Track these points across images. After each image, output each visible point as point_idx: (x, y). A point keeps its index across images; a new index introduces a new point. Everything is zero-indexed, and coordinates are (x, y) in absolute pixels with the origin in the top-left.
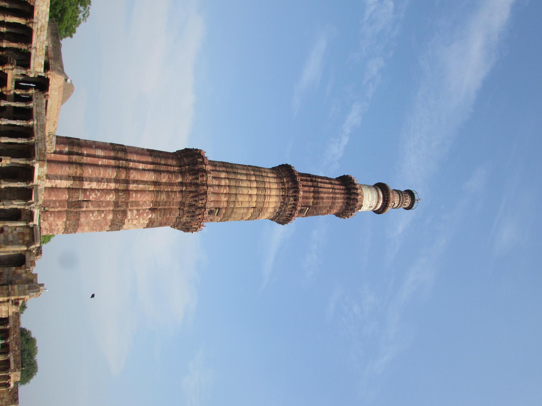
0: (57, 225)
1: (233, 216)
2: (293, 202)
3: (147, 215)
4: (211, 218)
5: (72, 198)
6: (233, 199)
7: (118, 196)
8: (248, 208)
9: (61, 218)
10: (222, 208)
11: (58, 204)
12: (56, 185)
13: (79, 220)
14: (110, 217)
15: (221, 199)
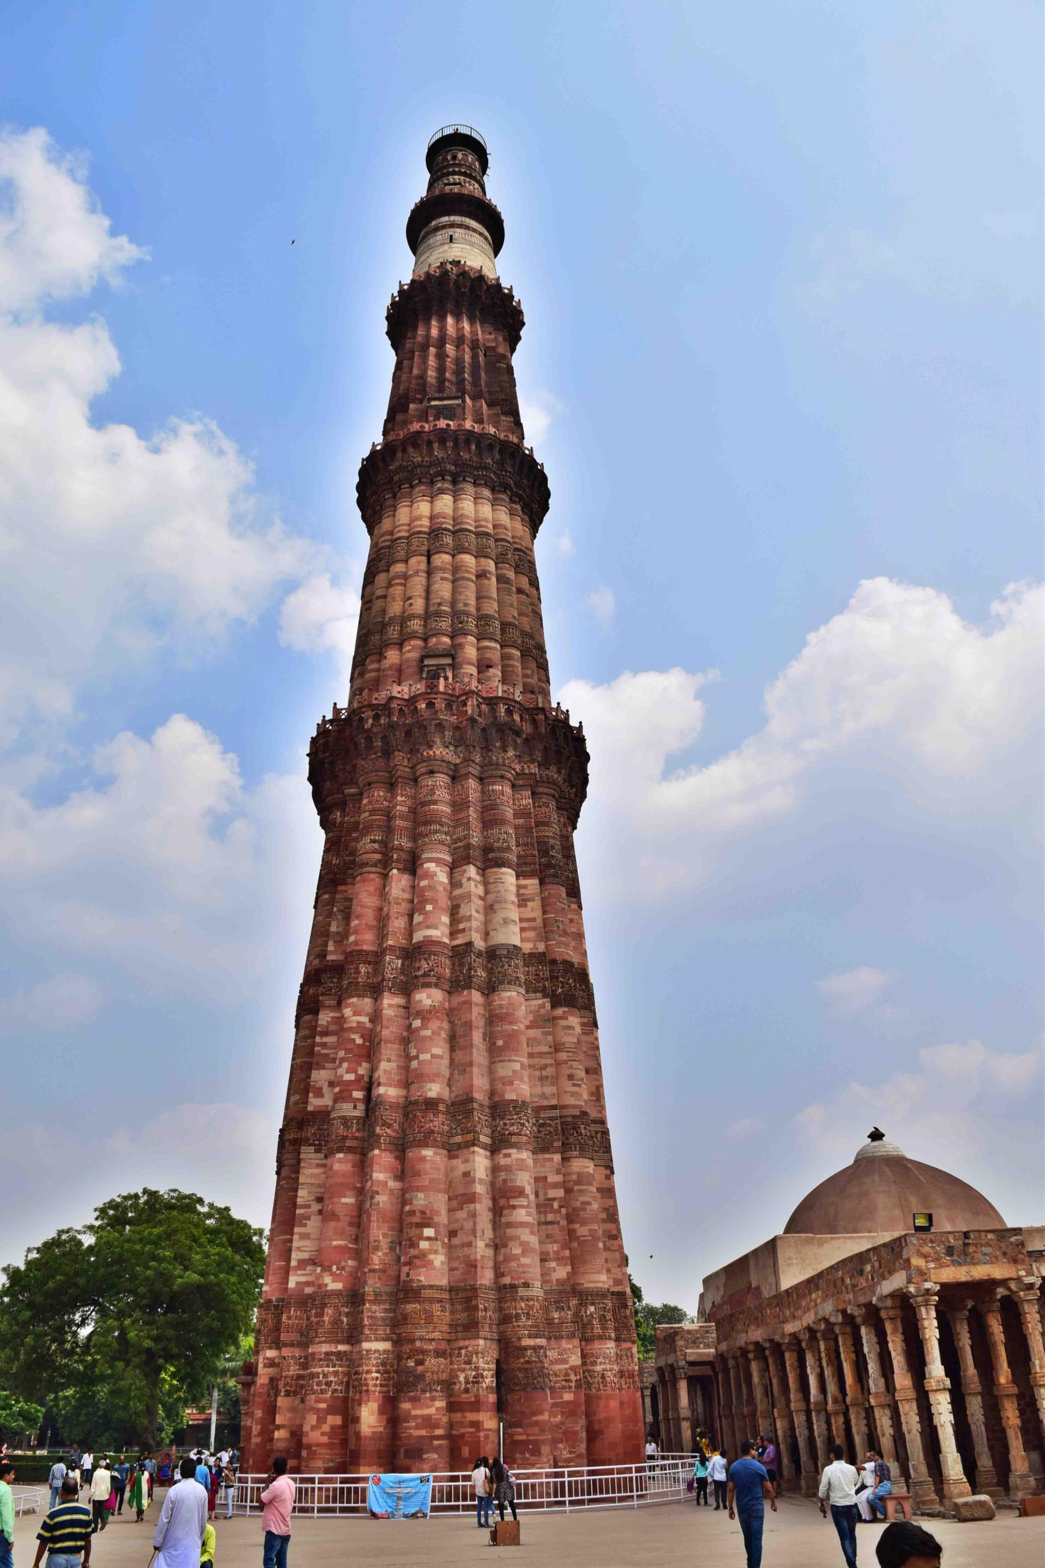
0: (467, 1174)
1: (460, 606)
2: (399, 454)
3: (429, 875)
4: (474, 671)
5: (344, 1138)
6: (393, 633)
7: (347, 989)
8: (429, 573)
9: (419, 1166)
10: (425, 647)
11: (369, 1183)
12: (320, 1200)
13: (431, 1104)
14: (427, 998)
15: (390, 668)
